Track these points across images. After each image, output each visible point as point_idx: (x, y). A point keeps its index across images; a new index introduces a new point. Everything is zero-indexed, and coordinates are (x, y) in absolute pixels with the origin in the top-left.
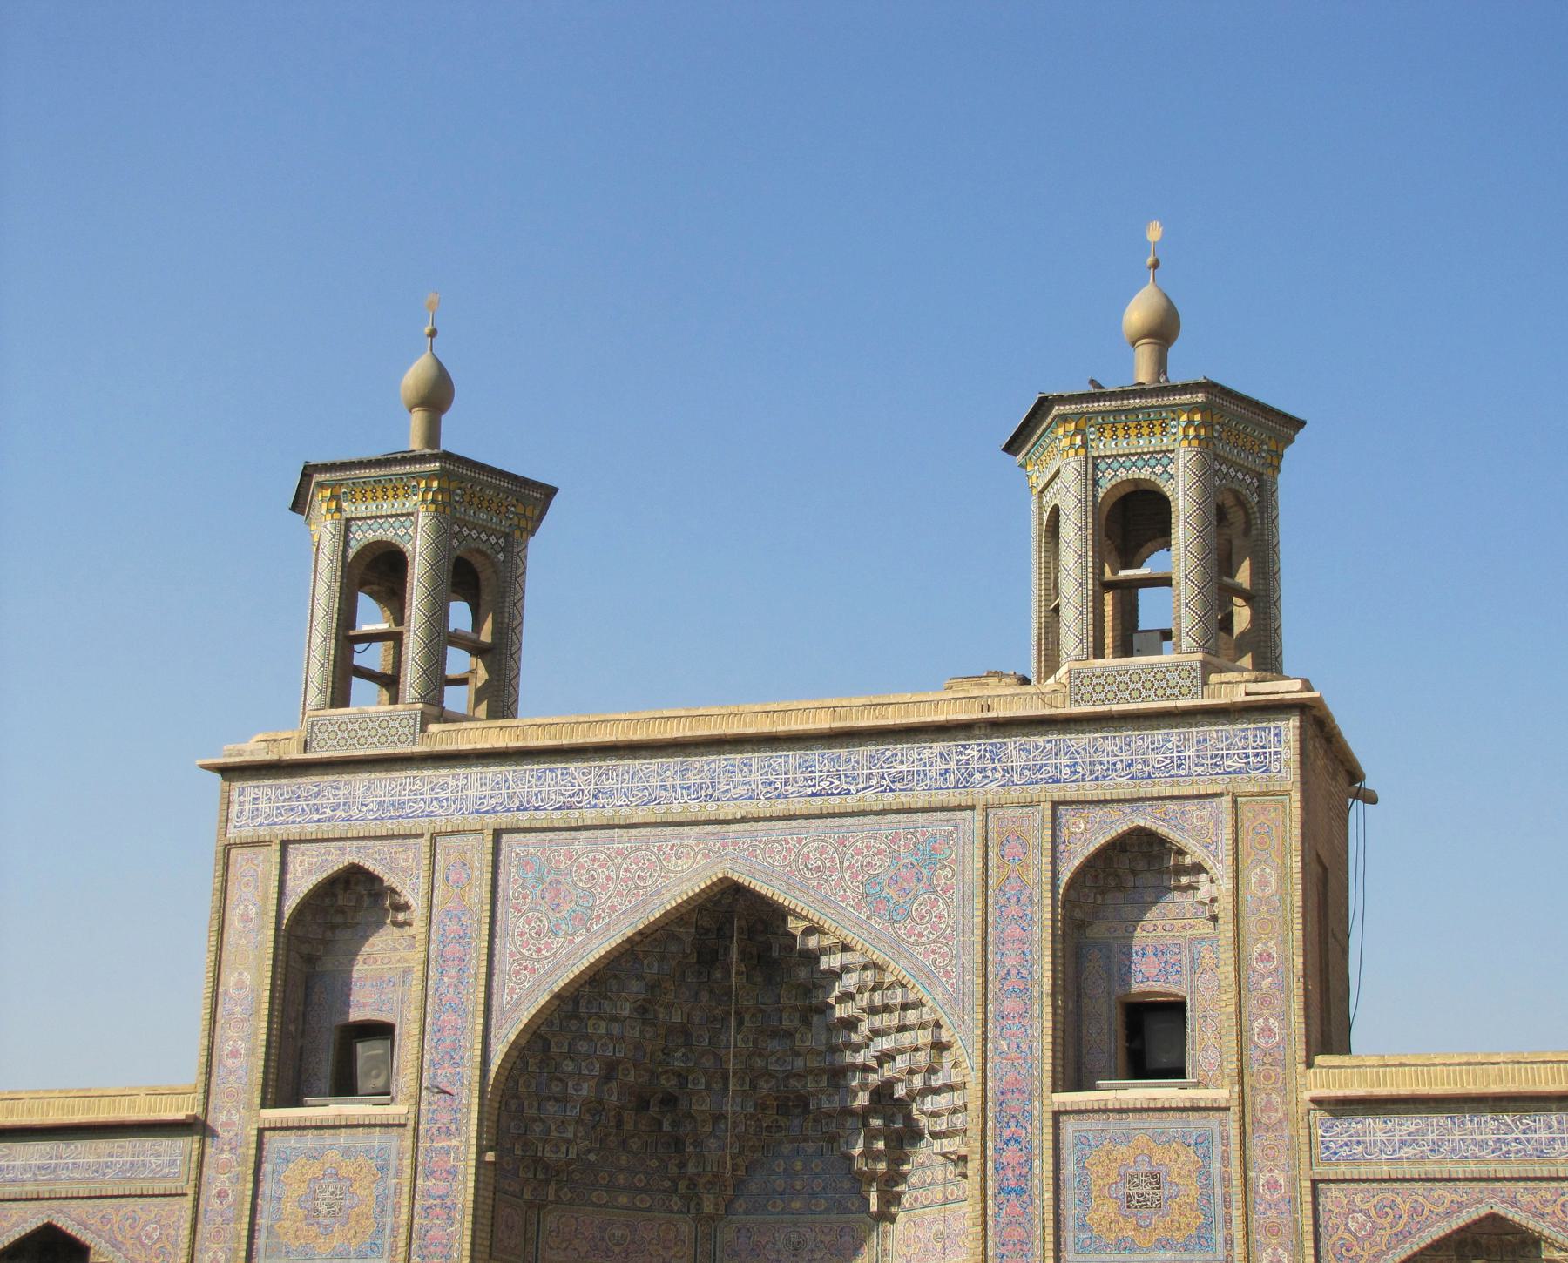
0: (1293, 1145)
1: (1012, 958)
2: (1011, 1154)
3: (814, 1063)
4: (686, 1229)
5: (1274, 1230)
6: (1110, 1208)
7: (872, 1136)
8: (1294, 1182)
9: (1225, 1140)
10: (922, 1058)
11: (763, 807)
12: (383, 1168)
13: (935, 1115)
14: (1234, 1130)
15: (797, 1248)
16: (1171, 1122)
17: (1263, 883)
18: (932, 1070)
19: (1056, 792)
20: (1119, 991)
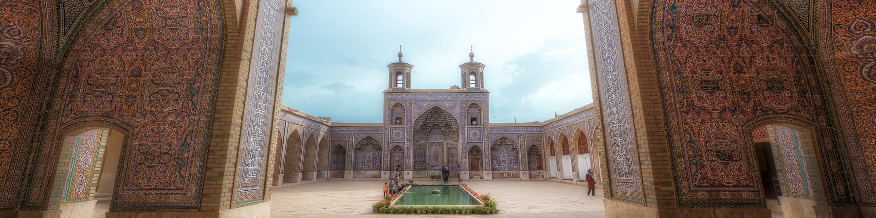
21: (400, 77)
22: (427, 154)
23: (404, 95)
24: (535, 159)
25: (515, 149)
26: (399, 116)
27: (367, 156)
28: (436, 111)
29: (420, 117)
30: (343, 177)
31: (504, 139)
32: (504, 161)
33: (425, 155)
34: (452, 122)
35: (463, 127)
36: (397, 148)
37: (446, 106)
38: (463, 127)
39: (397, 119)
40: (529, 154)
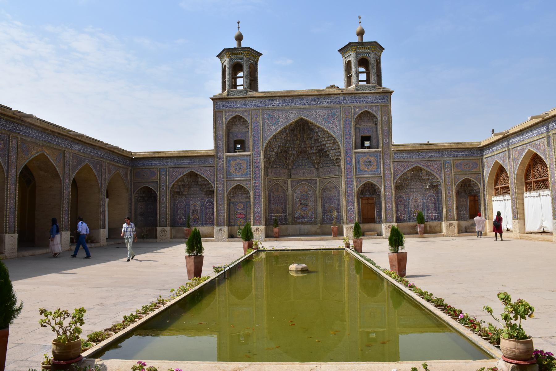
0: (390, 157)
1: (347, 130)
2: (348, 159)
3: (309, 146)
4: (286, 171)
5: (387, 169)
6: (363, 166)
7: (316, 157)
8: (390, 162)
9: (380, 156)
10: (331, 145)
11: (306, 105)
12: (247, 162)
13: (333, 153)
14: (381, 155)
15: (303, 173)
16: (372, 154)
17: (385, 119)
18: (332, 147)
19: (354, 104)
20: (361, 135)
21: (240, 74)
22: (290, 199)
23: (247, 102)
24: (466, 202)
25: (435, 187)
26: (240, 137)
27: (192, 203)
28: (302, 127)
29: (275, 137)
30: (156, 237)
31: (419, 166)
32: (416, 207)
33: (285, 201)
34: (329, 144)
35: (347, 152)
36: (240, 190)
37: (316, 118)
38: (347, 152)
39: (236, 142)
40: (458, 194)
